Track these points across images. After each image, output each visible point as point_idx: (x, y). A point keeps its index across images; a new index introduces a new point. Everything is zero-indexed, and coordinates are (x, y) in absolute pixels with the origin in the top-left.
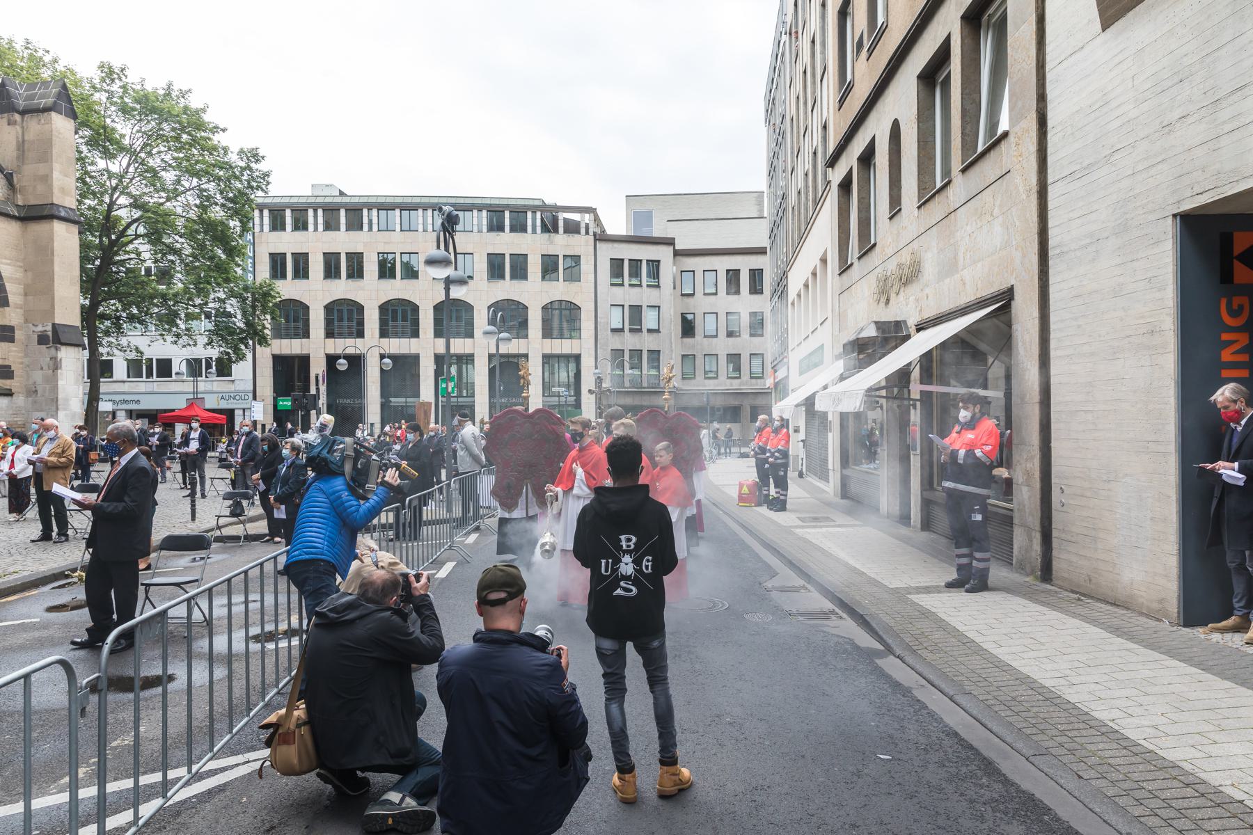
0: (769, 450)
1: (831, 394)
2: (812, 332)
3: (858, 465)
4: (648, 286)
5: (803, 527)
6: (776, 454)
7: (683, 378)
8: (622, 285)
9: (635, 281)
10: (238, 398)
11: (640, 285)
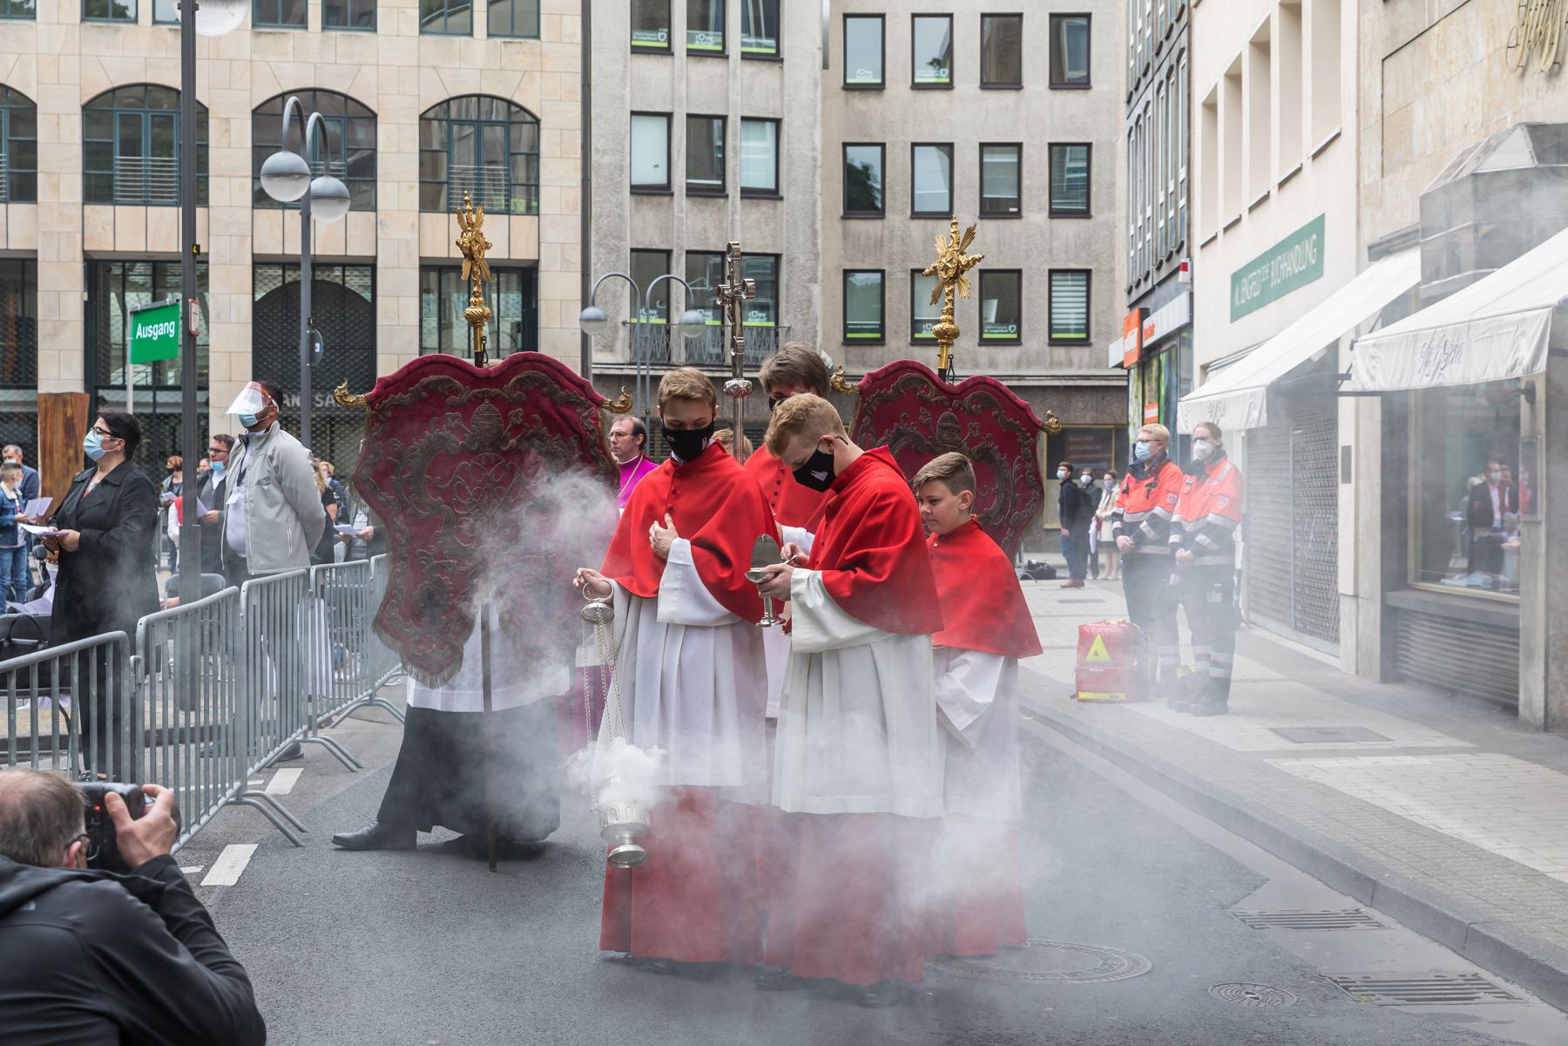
0: (1178, 525)
1: (1415, 336)
2: (1282, 185)
3: (1437, 579)
4: (746, 57)
5: (1296, 755)
6: (1201, 538)
7: (847, 342)
8: (667, 51)
9: (708, 42)
11: (722, 55)
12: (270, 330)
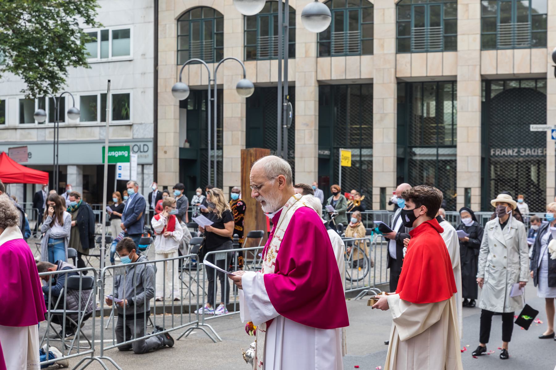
12: (497, 115)
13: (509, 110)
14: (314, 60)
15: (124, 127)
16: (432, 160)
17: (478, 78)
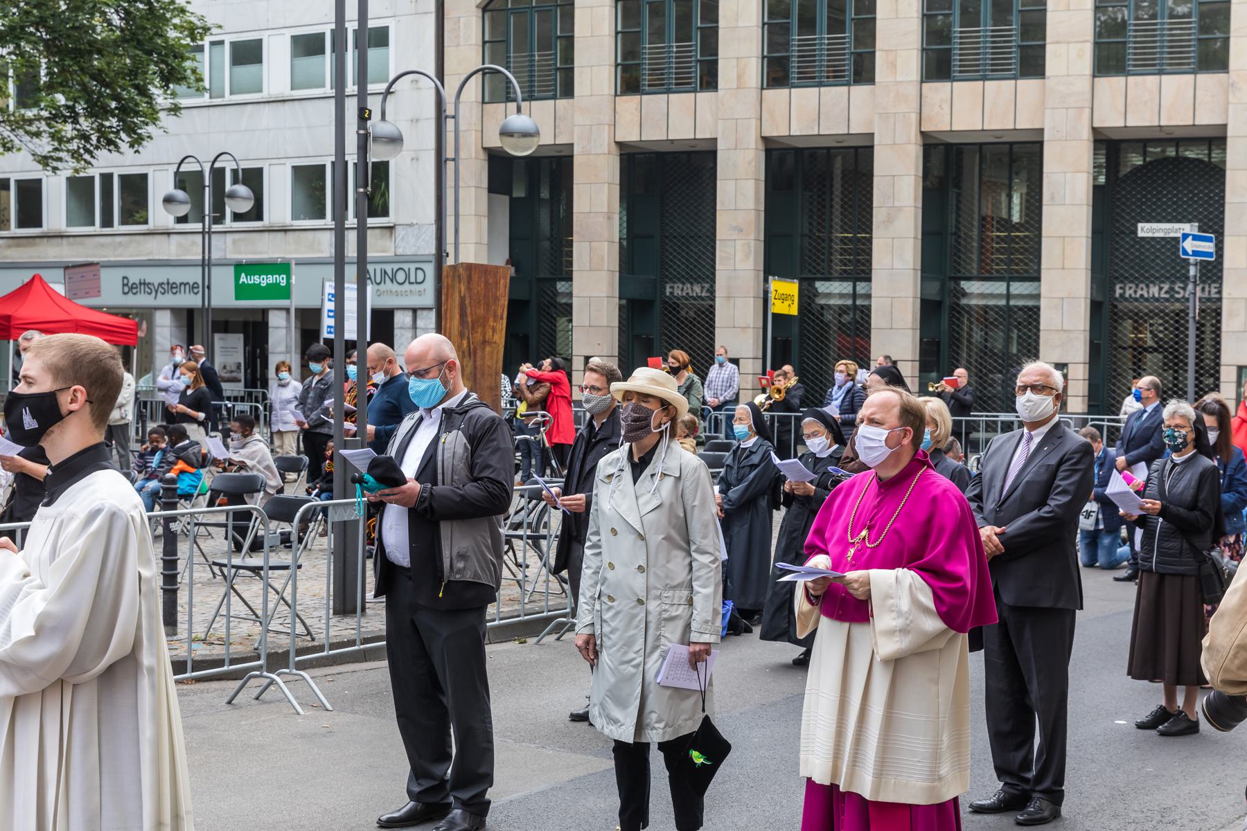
10: (401, 276)
13: (1154, 203)
14: (754, 94)
15: (377, 231)
16: (997, 306)
17: (1086, 135)
